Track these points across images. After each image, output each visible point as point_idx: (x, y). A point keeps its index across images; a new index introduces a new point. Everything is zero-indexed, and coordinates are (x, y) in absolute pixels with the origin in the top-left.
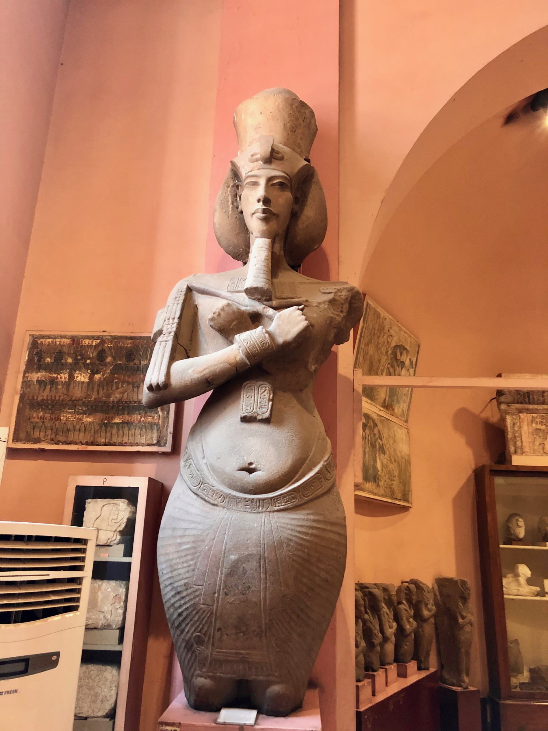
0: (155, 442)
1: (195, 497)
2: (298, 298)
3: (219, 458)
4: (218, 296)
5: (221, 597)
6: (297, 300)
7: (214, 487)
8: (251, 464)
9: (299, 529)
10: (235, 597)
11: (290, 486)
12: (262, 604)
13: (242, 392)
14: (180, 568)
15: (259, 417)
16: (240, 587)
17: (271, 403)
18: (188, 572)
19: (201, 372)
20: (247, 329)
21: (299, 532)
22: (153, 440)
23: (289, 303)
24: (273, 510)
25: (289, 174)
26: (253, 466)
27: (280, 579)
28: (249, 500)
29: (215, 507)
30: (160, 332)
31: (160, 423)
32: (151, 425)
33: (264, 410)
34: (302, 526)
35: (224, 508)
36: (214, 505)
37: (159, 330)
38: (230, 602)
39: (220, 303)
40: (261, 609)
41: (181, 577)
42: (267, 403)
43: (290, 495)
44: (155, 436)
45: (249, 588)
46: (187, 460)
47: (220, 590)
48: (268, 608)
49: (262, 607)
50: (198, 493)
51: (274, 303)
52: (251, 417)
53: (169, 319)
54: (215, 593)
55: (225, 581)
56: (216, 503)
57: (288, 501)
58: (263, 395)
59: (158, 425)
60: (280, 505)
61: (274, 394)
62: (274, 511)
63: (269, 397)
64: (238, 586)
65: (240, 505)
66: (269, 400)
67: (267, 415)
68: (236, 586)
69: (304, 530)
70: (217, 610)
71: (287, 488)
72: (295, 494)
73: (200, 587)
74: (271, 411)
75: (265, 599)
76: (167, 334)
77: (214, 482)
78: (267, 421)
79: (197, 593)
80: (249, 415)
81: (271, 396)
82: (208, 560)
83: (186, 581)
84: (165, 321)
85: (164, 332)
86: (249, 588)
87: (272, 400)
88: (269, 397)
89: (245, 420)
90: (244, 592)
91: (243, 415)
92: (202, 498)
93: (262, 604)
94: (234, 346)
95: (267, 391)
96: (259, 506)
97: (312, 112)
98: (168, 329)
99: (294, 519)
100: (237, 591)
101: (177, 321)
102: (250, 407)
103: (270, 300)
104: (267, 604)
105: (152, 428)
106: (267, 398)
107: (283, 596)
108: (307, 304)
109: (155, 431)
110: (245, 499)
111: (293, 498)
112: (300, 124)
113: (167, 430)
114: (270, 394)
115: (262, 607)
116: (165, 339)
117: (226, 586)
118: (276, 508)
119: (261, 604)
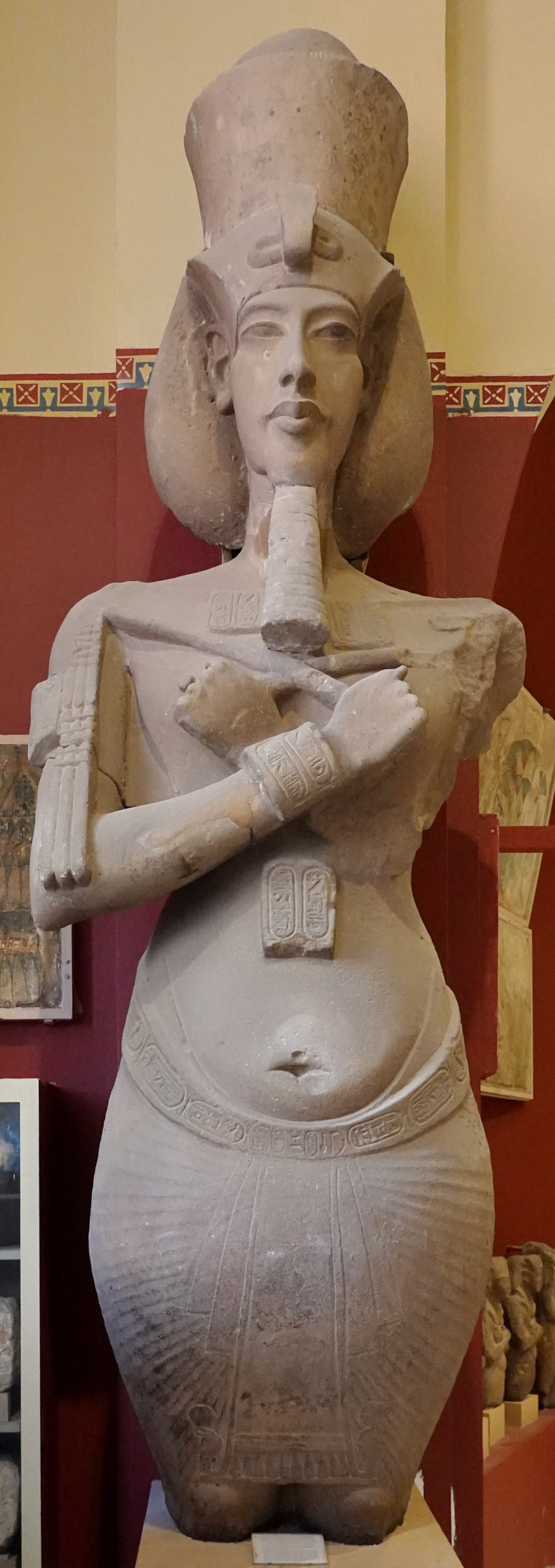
0: (34, 997)
1: (174, 1129)
2: (386, 645)
3: (222, 1043)
4: (187, 644)
5: (247, 1334)
6: (383, 652)
7: (217, 1106)
8: (296, 1054)
9: (409, 1190)
10: (279, 1333)
11: (385, 1099)
12: (336, 1344)
13: (264, 886)
14: (156, 1279)
15: (308, 947)
16: (289, 1313)
17: (332, 912)
18: (173, 1286)
19: (169, 841)
20: (270, 731)
21: (411, 1197)
22: (29, 994)
23: (368, 661)
24: (352, 1152)
25: (351, 294)
26: (302, 1059)
27: (373, 1294)
28: (299, 1132)
29: (224, 1151)
30: (53, 741)
31: (42, 951)
32: (22, 958)
33: (318, 929)
34: (414, 1183)
35: (244, 1151)
36: (221, 1145)
37: (48, 737)
38: (269, 1341)
39: (200, 667)
40: (333, 1353)
41: (158, 1296)
42: (324, 912)
43: (386, 1119)
44: (33, 983)
45: (309, 1313)
46: (142, 1046)
47: (246, 1321)
48: (347, 1351)
49: (336, 1350)
50: (180, 1119)
51: (334, 660)
52: (289, 945)
53: (69, 706)
54: (233, 1328)
55: (256, 1304)
56: (224, 1141)
57: (383, 1133)
58: (312, 893)
59: (36, 958)
60: (366, 1141)
61: (339, 888)
62: (355, 1155)
63: (329, 896)
64: (285, 1312)
65: (280, 1144)
66: (328, 904)
67: (327, 941)
68: (281, 1309)
69: (420, 1191)
70: (240, 1359)
71: (380, 1103)
72: (399, 1115)
73: (203, 1316)
74: (335, 931)
75: (342, 1334)
76: (73, 747)
77: (216, 1096)
78: (328, 954)
79: (196, 1329)
80: (284, 941)
81: (333, 894)
82: (218, 1262)
83: (170, 1304)
84: (60, 712)
85: (62, 741)
86: (309, 1313)
87: (335, 906)
88: (329, 896)
89: (274, 953)
90: (297, 1323)
91: (270, 944)
92: (190, 1131)
93: (336, 1344)
94: (241, 776)
95: (322, 881)
96: (321, 1146)
97: (402, 109)
98: (72, 732)
99: (399, 1168)
100: (282, 1320)
101: (92, 713)
102: (284, 921)
103: (318, 653)
104: (347, 1344)
105: (26, 969)
106: (325, 901)
107: (380, 1328)
108: (408, 660)
109: (32, 972)
110: (291, 1130)
111: (394, 1125)
112: (372, 148)
113: (58, 970)
114: (329, 889)
115: (336, 1350)
116: (67, 758)
117: (260, 1312)
118: (359, 1149)
119: (333, 1345)
